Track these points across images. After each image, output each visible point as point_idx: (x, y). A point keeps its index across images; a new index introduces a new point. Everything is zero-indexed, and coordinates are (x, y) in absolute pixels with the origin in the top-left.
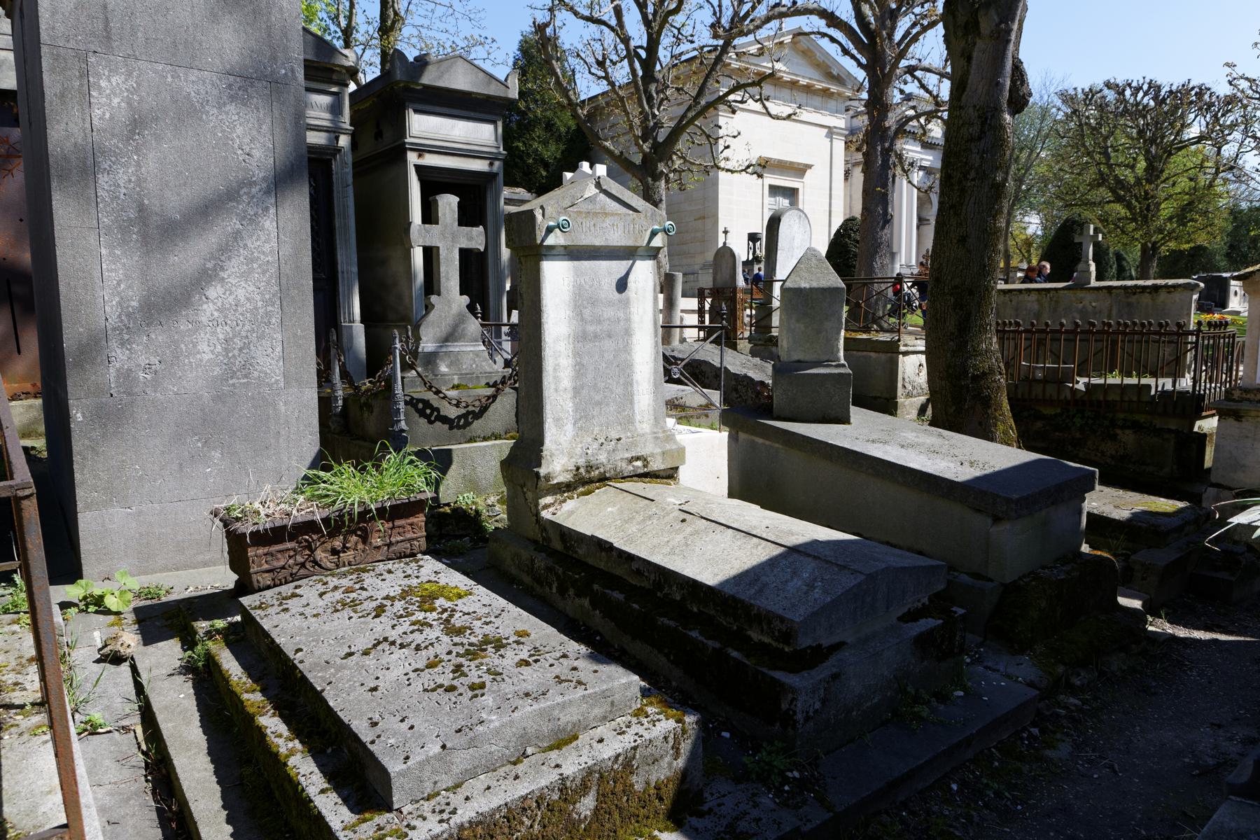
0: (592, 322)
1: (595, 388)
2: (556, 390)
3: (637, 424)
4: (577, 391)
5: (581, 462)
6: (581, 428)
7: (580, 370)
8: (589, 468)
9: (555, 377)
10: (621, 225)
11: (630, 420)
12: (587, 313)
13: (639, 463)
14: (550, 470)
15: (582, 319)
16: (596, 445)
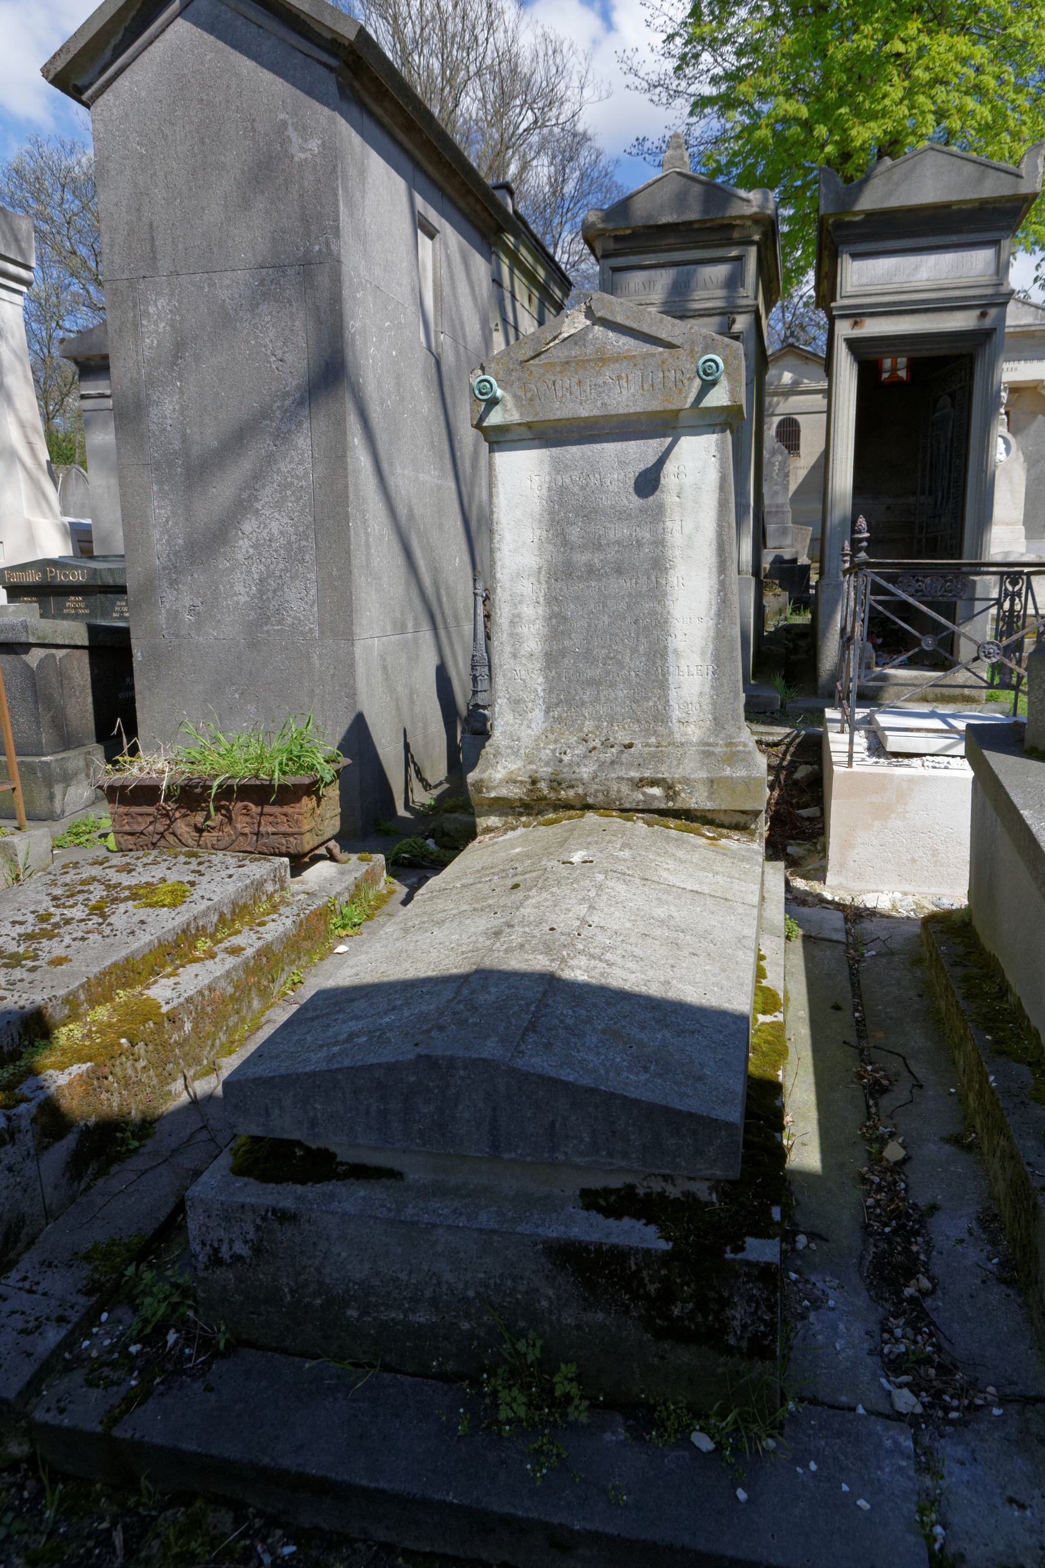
0: (583, 548)
1: (587, 656)
2: (515, 656)
3: (675, 726)
4: (552, 660)
5: (545, 771)
6: (559, 720)
7: (557, 625)
8: (556, 783)
9: (511, 635)
10: (636, 375)
11: (660, 717)
12: (575, 533)
13: (656, 791)
14: (485, 776)
15: (565, 543)
16: (580, 750)
